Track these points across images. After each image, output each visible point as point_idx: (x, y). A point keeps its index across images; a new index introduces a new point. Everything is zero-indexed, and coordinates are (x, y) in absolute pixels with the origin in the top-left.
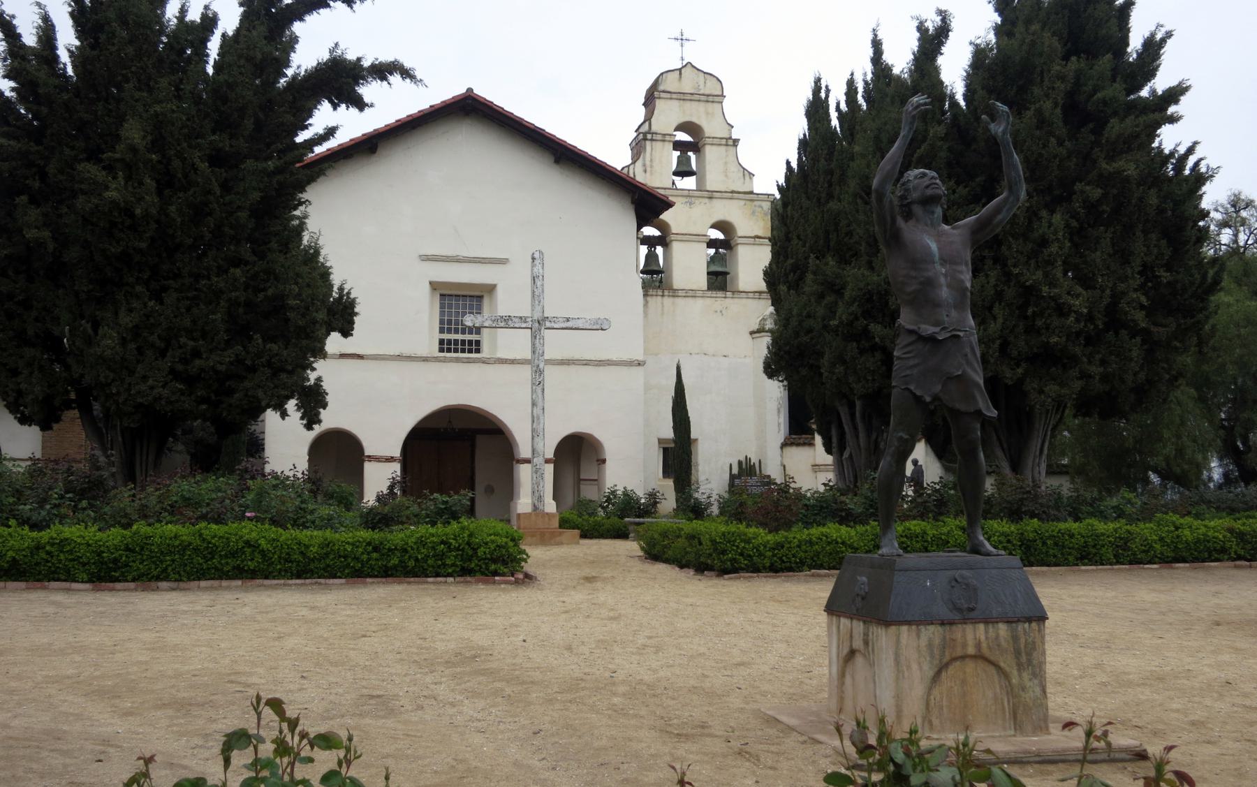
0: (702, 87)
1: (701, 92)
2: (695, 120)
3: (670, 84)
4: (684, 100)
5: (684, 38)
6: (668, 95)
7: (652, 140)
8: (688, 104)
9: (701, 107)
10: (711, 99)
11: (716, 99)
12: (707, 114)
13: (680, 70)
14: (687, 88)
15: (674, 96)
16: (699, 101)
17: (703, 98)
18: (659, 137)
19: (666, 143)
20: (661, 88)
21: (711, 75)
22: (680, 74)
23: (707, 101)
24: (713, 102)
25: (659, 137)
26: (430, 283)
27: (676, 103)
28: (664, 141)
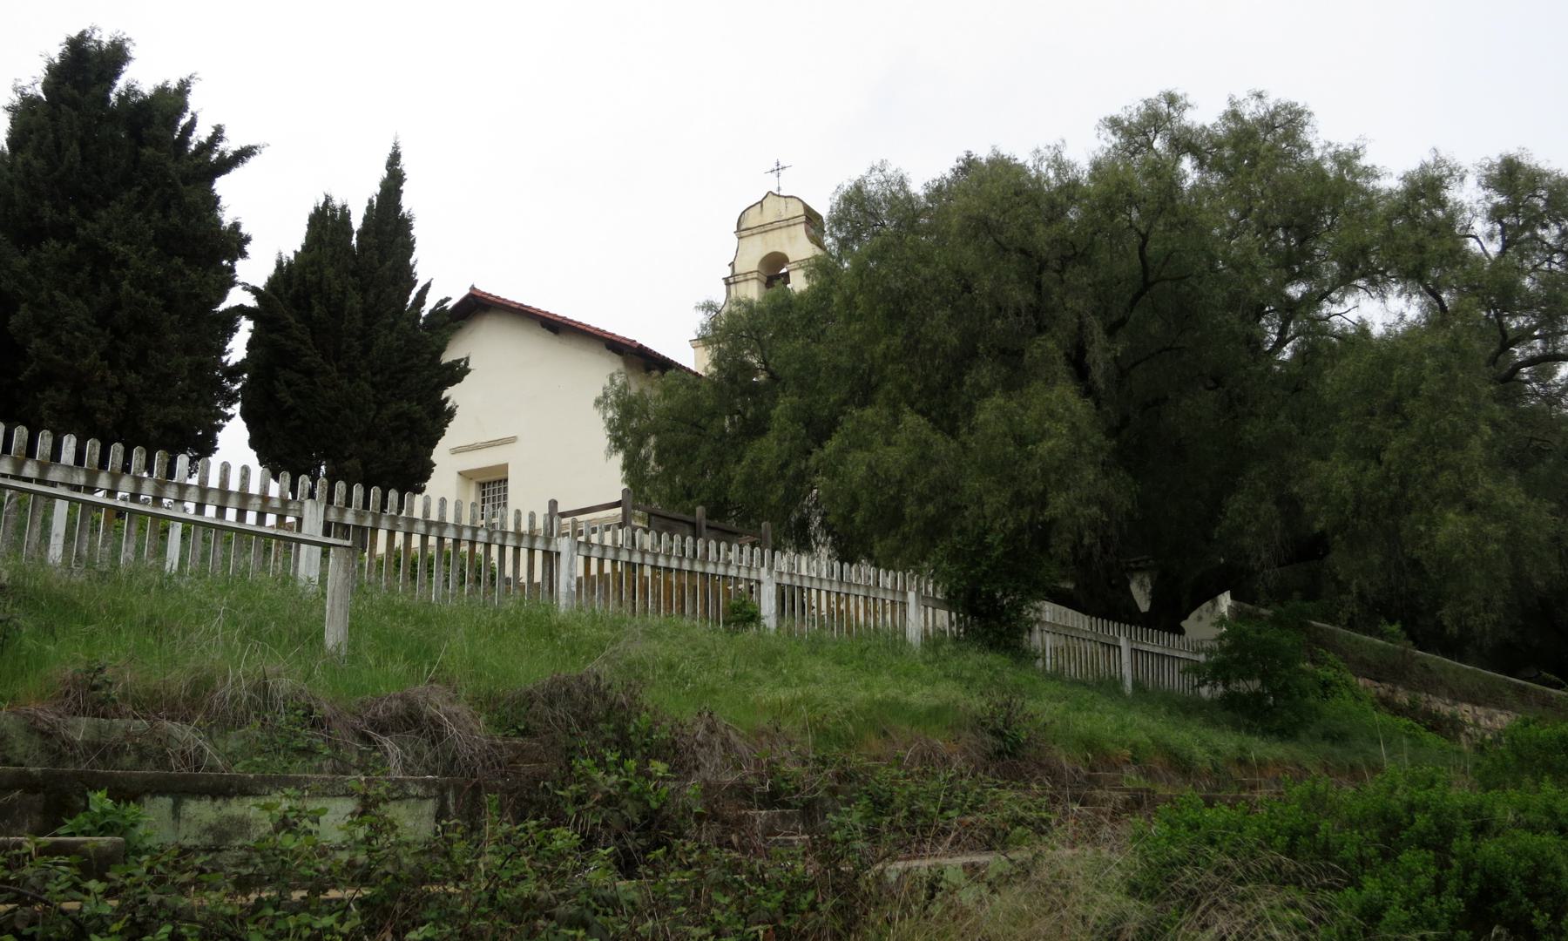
0: (783, 212)
1: (784, 218)
2: (778, 249)
3: (753, 220)
4: (766, 232)
5: (776, 168)
6: (749, 232)
7: (735, 283)
8: (770, 235)
9: (784, 233)
10: (791, 222)
11: (797, 220)
12: (790, 238)
13: (761, 202)
14: (769, 216)
15: (755, 231)
16: (780, 228)
17: (782, 224)
18: (741, 278)
19: (750, 282)
20: (743, 227)
21: (791, 197)
22: (762, 206)
23: (789, 226)
24: (794, 225)
25: (741, 278)
26: (460, 473)
27: (758, 238)
28: (747, 280)
